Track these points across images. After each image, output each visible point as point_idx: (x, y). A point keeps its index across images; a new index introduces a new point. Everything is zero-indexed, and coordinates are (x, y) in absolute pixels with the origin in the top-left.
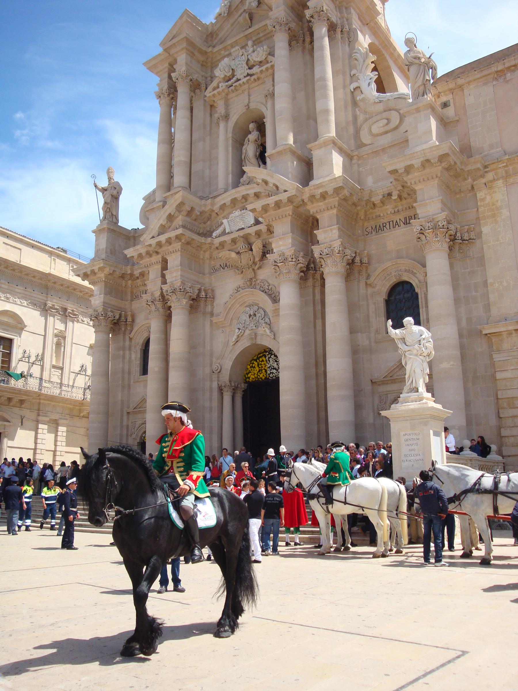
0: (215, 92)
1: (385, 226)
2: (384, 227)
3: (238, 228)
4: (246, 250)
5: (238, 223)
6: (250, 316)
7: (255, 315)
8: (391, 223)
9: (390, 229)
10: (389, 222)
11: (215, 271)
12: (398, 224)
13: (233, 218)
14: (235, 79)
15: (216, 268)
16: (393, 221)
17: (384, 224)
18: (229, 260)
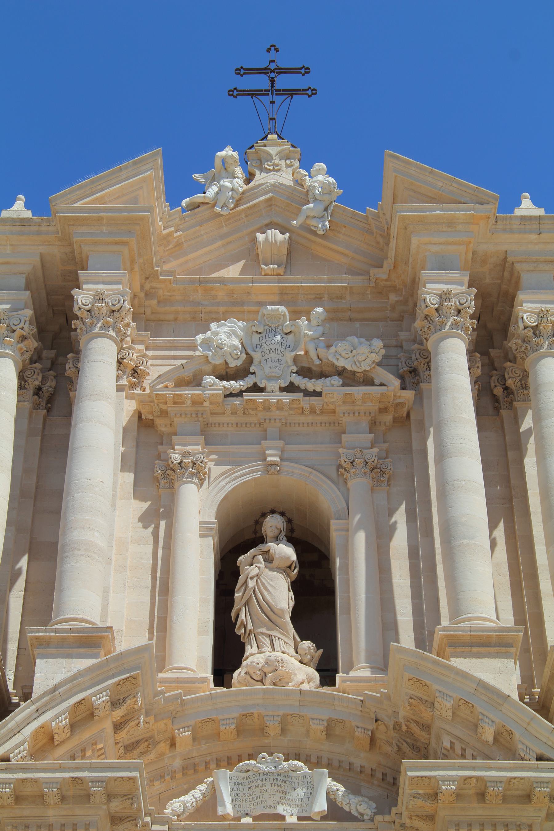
0: (188, 392)
5: (266, 795)
14: (248, 382)
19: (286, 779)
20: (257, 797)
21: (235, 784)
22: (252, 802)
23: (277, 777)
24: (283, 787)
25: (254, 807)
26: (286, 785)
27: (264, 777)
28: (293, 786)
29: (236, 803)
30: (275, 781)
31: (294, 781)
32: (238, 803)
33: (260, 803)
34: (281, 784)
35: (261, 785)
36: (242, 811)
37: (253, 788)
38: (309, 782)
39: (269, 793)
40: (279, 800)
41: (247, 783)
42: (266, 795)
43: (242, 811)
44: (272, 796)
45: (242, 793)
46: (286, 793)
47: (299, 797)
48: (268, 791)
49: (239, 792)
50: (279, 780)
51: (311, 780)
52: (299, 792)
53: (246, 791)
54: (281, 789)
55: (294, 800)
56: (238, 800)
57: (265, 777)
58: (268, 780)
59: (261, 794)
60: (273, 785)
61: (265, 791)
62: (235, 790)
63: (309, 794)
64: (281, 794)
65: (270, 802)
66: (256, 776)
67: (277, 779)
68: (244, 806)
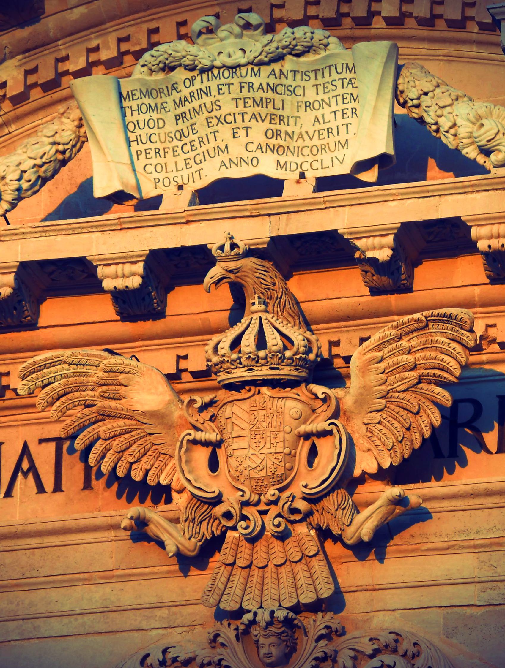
5: (225, 132)
13: (180, 75)
19: (277, 81)
20: (201, 141)
21: (139, 109)
22: (192, 154)
23: (249, 79)
24: (270, 106)
25: (196, 168)
26: (277, 97)
27: (213, 84)
28: (300, 99)
29: (149, 161)
30: (245, 90)
31: (302, 84)
32: (154, 161)
33: (212, 154)
34: (264, 95)
35: (209, 105)
36: (166, 182)
37: (188, 116)
38: (346, 82)
39: (233, 125)
40: (263, 140)
41: (170, 105)
43: (166, 182)
44: (242, 133)
45: (162, 131)
46: (281, 118)
47: (322, 126)
48: (230, 119)
49: (152, 131)
50: (256, 86)
51: (352, 75)
52: (319, 113)
53: (171, 127)
54: (264, 111)
55: (306, 137)
56: (152, 153)
57: (217, 82)
58: (225, 89)
59: (210, 130)
60: (241, 103)
62: (142, 126)
63: (349, 113)
64: (266, 125)
66: (192, 81)
67: (251, 86)
68: (171, 166)
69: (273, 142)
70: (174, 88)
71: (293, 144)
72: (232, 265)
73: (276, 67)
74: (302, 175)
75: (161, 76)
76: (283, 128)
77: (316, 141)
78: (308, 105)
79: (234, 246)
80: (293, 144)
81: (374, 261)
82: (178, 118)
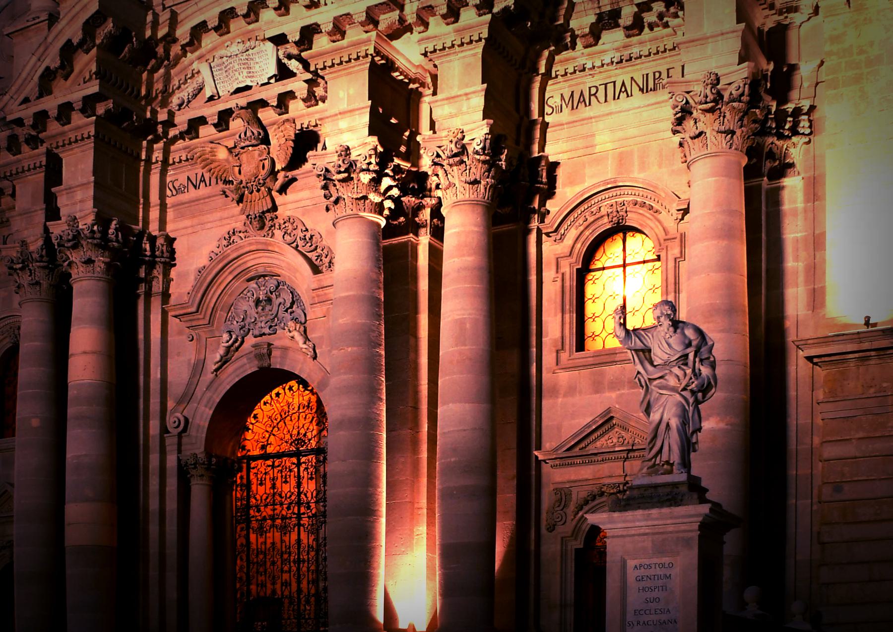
1: (594, 95)
2: (593, 98)
3: (236, 86)
4: (254, 142)
5: (237, 73)
6: (258, 302)
7: (269, 300)
8: (610, 86)
9: (606, 101)
10: (606, 85)
11: (174, 193)
12: (626, 90)
13: (225, 59)
15: (177, 185)
16: (614, 82)
17: (593, 91)
18: (212, 166)
27: (232, 61)
40: (247, 75)
42: (237, 73)
53: (225, 75)
54: (245, 66)
61: (236, 71)
64: (247, 70)
65: (240, 79)
66: (227, 60)
69: (249, 75)
70: (224, 63)
71: (255, 75)
72: (238, 112)
73: (247, 53)
74: (258, 83)
75: (220, 60)
76: (251, 71)
77: (260, 73)
78: (257, 63)
79: (237, 107)
80: (255, 75)
81: (273, 106)
82: (226, 71)
